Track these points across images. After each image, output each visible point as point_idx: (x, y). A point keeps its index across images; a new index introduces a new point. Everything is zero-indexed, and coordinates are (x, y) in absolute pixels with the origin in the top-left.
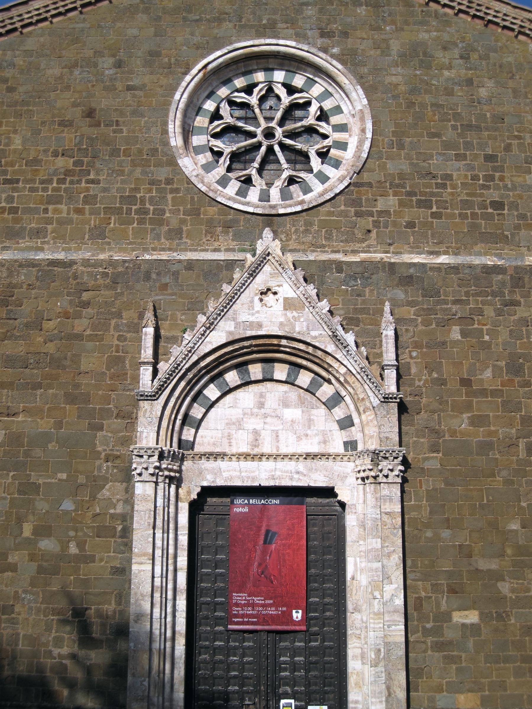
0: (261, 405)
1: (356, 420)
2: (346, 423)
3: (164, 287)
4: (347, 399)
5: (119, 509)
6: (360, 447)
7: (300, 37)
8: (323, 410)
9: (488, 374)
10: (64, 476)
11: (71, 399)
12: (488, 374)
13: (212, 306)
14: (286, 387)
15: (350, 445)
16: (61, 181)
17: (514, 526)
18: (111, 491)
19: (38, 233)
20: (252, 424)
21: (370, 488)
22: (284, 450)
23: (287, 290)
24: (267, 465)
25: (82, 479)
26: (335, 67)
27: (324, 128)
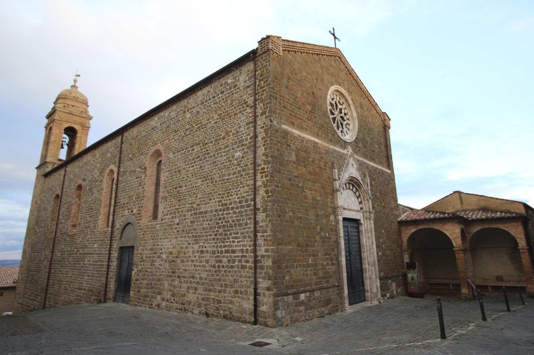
0: (348, 195)
1: (363, 202)
2: (360, 203)
3: (334, 157)
4: (362, 197)
5: (333, 223)
6: (364, 209)
7: (345, 89)
8: (356, 199)
9: (378, 194)
10: (323, 212)
11: (323, 188)
12: (378, 194)
13: (345, 166)
14: (351, 191)
15: (361, 209)
16: (309, 114)
17: (383, 231)
18: (332, 217)
19: (306, 130)
20: (347, 200)
21: (368, 221)
22: (353, 209)
23: (355, 166)
24: (351, 212)
25: (327, 214)
26: (351, 102)
27: (345, 118)
